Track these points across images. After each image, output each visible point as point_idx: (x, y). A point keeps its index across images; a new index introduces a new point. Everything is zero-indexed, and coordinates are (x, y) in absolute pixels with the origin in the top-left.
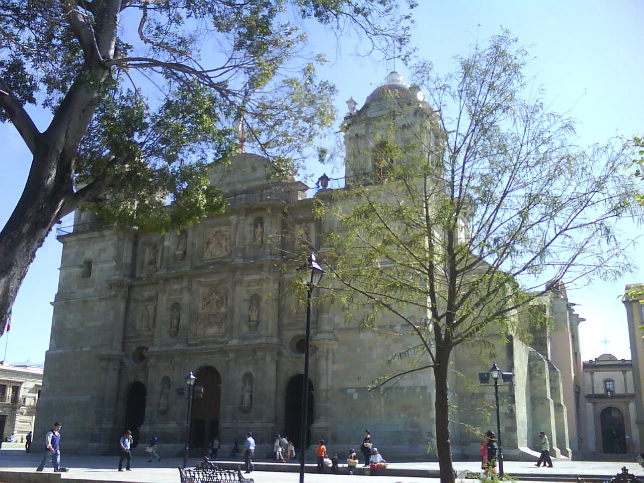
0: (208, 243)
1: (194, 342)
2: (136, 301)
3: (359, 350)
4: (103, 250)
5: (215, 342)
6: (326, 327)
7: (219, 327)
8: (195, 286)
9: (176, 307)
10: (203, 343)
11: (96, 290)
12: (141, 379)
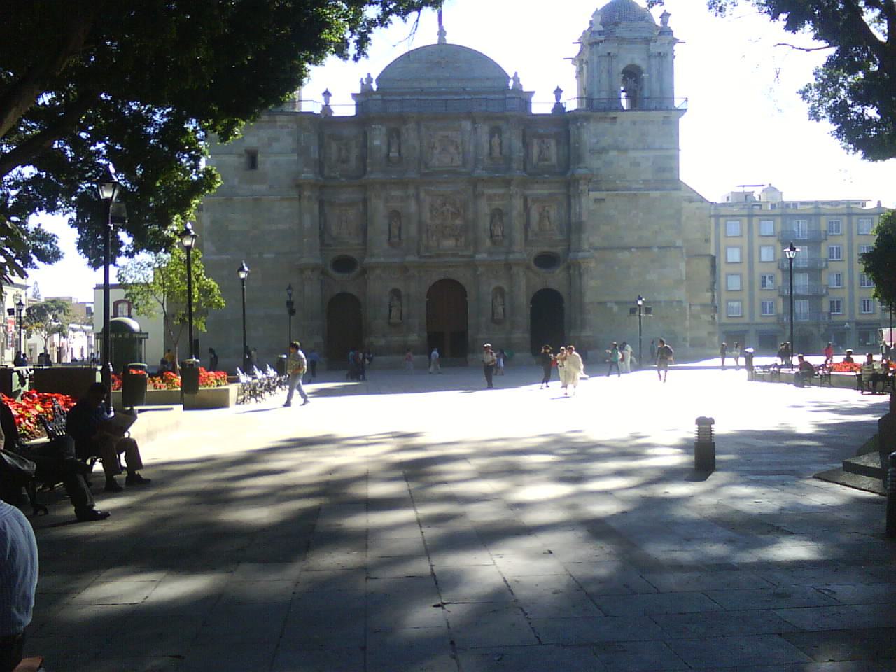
1: (427, 254)
4: (277, 140)
5: (455, 255)
6: (586, 247)
7: (457, 240)
8: (422, 195)
9: (395, 215)
10: (439, 256)
11: (271, 187)
12: (352, 290)
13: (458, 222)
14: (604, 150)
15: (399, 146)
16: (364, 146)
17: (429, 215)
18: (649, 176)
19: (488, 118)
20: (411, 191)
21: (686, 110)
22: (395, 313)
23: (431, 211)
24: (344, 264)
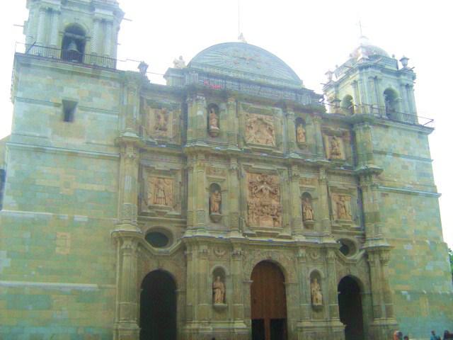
2: (150, 170)
3: (404, 258)
4: (99, 95)
9: (215, 188)
12: (169, 267)
14: (381, 153)
15: (218, 120)
16: (184, 117)
18: (415, 179)
19: (298, 108)
20: (234, 164)
21: (432, 129)
22: (219, 295)
23: (251, 189)
24: (158, 237)
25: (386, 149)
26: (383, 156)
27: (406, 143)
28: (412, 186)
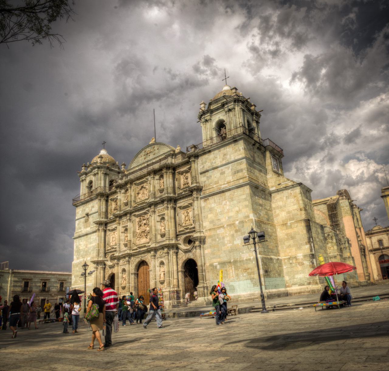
0: (138, 194)
3: (217, 240)
4: (93, 207)
7: (146, 238)
13: (148, 229)
17: (137, 228)
18: (230, 178)
25: (209, 167)
26: (207, 173)
27: (225, 155)
28: (227, 185)
